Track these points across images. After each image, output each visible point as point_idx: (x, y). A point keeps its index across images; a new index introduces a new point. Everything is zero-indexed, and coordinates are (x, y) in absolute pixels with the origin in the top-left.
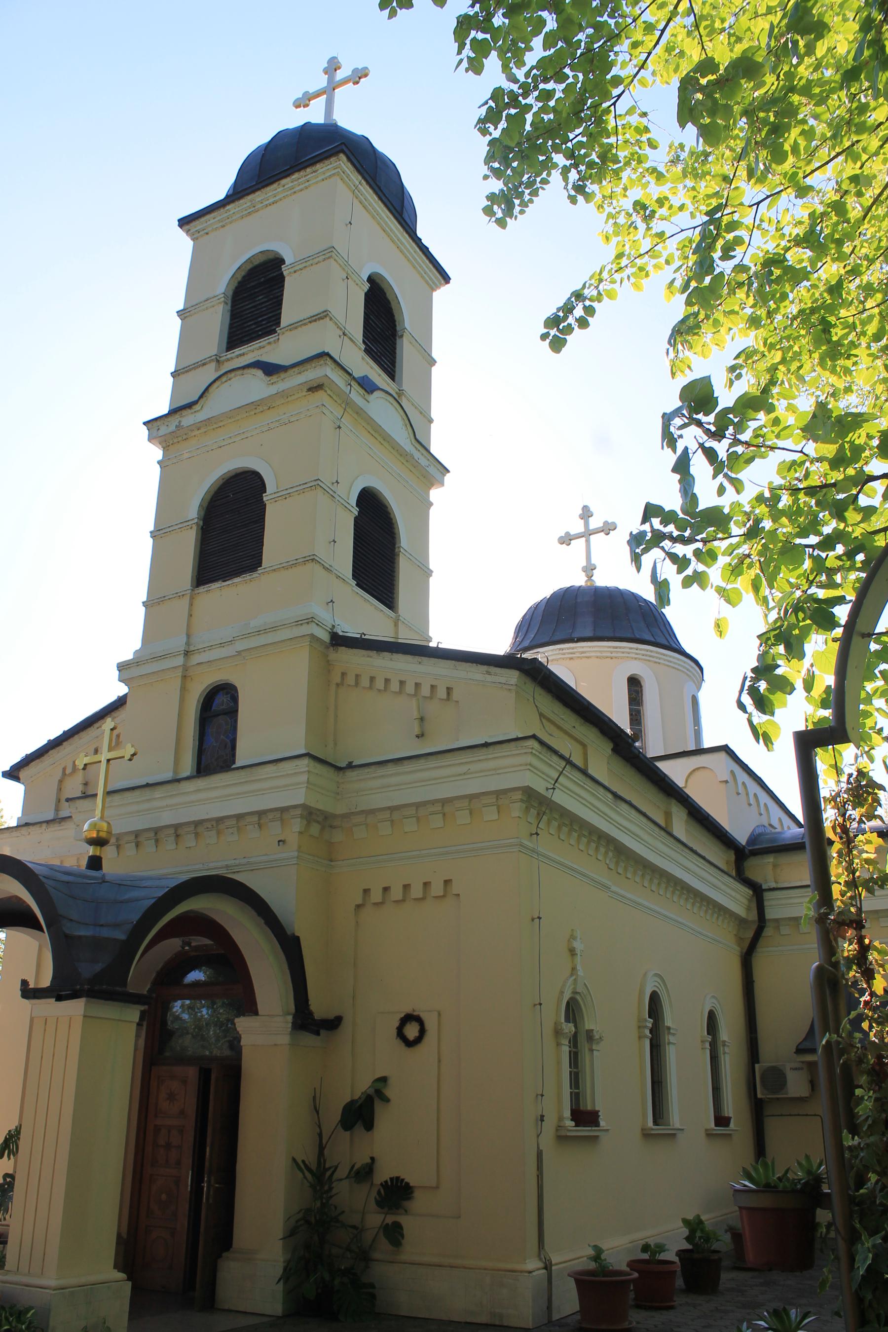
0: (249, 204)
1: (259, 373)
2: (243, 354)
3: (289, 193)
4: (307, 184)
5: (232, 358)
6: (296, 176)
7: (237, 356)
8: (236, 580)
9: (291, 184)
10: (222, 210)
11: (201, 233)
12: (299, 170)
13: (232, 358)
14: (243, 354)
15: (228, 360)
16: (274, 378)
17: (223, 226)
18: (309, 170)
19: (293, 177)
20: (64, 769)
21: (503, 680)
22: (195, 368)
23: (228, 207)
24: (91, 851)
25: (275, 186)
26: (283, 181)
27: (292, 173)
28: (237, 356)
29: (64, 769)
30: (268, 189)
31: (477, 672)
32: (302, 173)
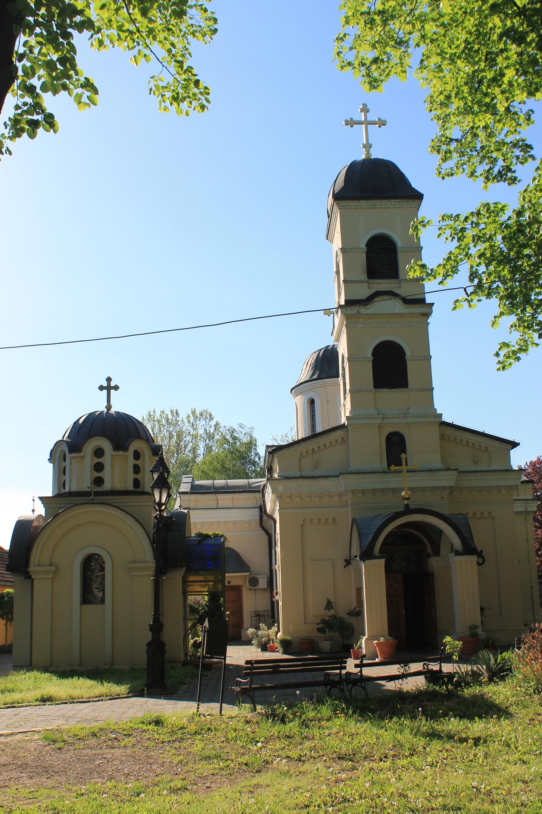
0: (372, 204)
1: (400, 301)
2: (380, 283)
3: (393, 206)
4: (402, 206)
5: (374, 283)
6: (398, 200)
7: (377, 283)
8: (396, 390)
9: (395, 203)
10: (358, 201)
11: (344, 207)
12: (400, 199)
13: (374, 283)
14: (380, 283)
15: (372, 283)
16: (408, 306)
17: (356, 208)
18: (405, 201)
19: (397, 201)
20: (301, 453)
21: (506, 448)
22: (356, 282)
23: (361, 201)
24: (406, 502)
25: (387, 201)
26: (392, 201)
27: (397, 199)
28: (377, 283)
29: (301, 453)
30: (384, 201)
31: (497, 444)
32: (401, 201)
